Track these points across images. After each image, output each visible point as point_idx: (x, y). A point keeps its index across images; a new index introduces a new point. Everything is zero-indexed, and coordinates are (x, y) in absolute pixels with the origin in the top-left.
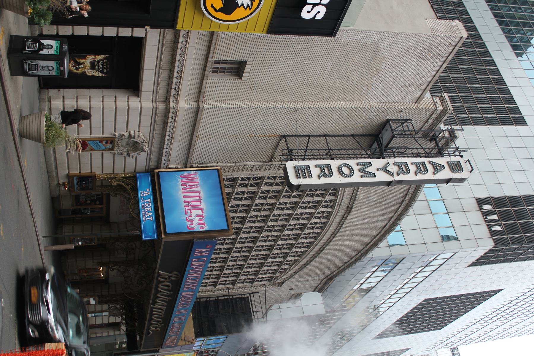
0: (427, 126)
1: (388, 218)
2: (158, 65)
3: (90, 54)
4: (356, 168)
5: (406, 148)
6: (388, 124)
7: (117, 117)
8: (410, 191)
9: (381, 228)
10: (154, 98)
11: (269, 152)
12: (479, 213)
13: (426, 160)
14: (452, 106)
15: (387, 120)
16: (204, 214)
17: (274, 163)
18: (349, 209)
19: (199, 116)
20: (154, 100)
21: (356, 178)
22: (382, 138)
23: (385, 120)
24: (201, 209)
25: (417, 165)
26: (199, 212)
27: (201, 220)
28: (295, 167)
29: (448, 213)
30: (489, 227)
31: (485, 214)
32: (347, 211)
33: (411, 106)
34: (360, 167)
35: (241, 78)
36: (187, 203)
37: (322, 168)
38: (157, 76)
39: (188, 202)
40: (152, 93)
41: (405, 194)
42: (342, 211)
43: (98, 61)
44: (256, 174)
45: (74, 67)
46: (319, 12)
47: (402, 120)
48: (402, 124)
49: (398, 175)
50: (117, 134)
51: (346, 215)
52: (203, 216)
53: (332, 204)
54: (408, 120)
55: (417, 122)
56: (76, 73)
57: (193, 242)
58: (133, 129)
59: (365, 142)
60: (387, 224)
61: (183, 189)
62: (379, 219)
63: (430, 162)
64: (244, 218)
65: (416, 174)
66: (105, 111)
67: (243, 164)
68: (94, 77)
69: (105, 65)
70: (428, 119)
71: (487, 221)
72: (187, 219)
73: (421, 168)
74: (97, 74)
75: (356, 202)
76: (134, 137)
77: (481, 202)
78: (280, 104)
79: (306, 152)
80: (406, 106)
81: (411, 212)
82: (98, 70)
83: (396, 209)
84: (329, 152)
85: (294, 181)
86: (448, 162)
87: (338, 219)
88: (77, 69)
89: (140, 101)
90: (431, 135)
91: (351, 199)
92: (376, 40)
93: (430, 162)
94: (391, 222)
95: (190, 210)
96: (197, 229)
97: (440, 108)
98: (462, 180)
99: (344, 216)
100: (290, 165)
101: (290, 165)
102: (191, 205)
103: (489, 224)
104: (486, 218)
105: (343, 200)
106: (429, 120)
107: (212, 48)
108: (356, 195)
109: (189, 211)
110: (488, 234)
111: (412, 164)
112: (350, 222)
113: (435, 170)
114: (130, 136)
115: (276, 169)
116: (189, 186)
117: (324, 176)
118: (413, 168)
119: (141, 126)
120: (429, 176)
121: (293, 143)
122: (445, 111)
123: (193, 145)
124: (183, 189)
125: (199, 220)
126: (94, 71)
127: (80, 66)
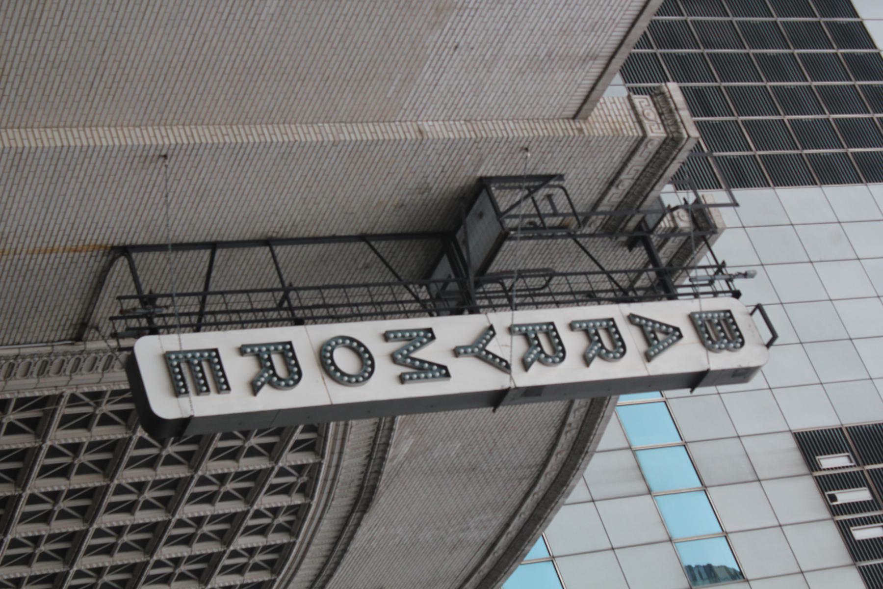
0: (615, 195)
1: (501, 517)
4: (380, 350)
5: (550, 274)
6: (484, 194)
8: (571, 419)
9: (479, 555)
11: (71, 309)
12: (808, 485)
13: (618, 312)
14: (699, 126)
15: (481, 179)
17: (91, 346)
18: (364, 496)
21: (384, 385)
22: (466, 242)
25: (589, 331)
28: (166, 357)
29: (704, 488)
30: (844, 529)
31: (828, 484)
32: (357, 500)
33: (562, 128)
34: (393, 346)
37: (260, 355)
41: (553, 431)
47: (530, 178)
48: (532, 191)
49: (526, 366)
51: (355, 516)
53: (304, 478)
54: (550, 177)
55: (582, 184)
59: (408, 258)
60: (498, 538)
62: (472, 525)
63: (631, 318)
64: (75, 538)
65: (587, 361)
71: (835, 510)
73: (603, 341)
75: (388, 467)
77: (812, 445)
78: (105, 137)
79: (203, 303)
80: (540, 130)
81: (578, 491)
83: (525, 485)
84: (286, 297)
85: (165, 405)
86: (691, 317)
90: (632, 224)
91: (370, 457)
93: (631, 318)
97: (656, 132)
98: (741, 375)
99: (347, 519)
100: (149, 350)
101: (149, 350)
103: (844, 518)
104: (833, 498)
105: (344, 464)
106: (623, 176)
108: (387, 444)
110: (841, 554)
111: (572, 326)
112: (369, 541)
113: (649, 342)
115: (101, 365)
117: (270, 383)
118: (574, 343)
120: (631, 365)
121: (155, 272)
122: (672, 142)
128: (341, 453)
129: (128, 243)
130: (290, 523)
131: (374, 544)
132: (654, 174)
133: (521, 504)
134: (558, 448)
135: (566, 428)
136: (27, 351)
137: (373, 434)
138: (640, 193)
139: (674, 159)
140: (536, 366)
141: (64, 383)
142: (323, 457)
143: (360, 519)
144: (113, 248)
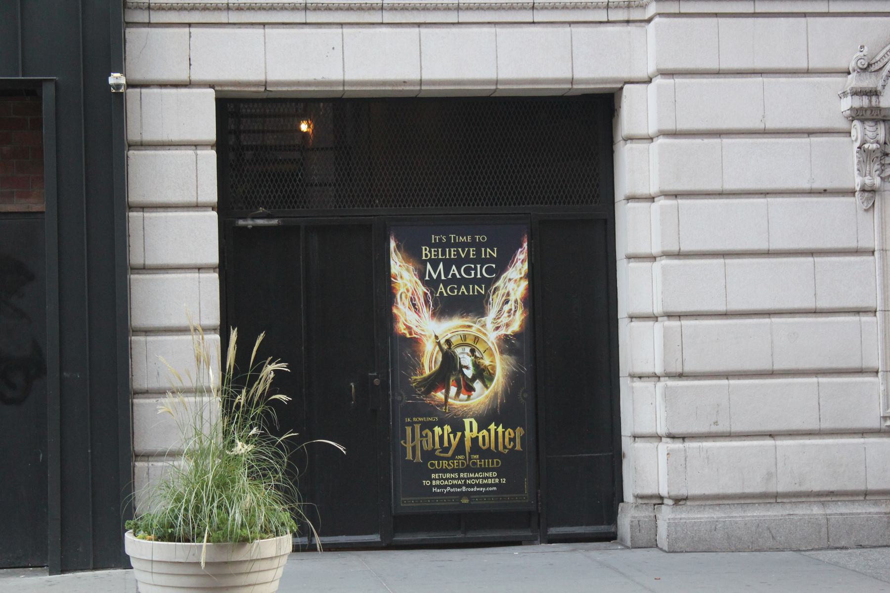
2: (388, 17)
3: (392, 319)
7: (729, 186)
10: (621, 15)
20: (636, 15)
38: (465, 17)
40: (499, 30)
43: (431, 284)
45: (470, 389)
50: (857, 182)
56: (514, 380)
58: (832, 103)
66: (686, 247)
68: (532, 300)
69: (452, 253)
74: (514, 282)
76: (873, 93)
82: (489, 283)
88: (483, 374)
89: (649, 81)
114: (858, 115)
119: (803, 65)
126: (496, 301)
127: (466, 360)
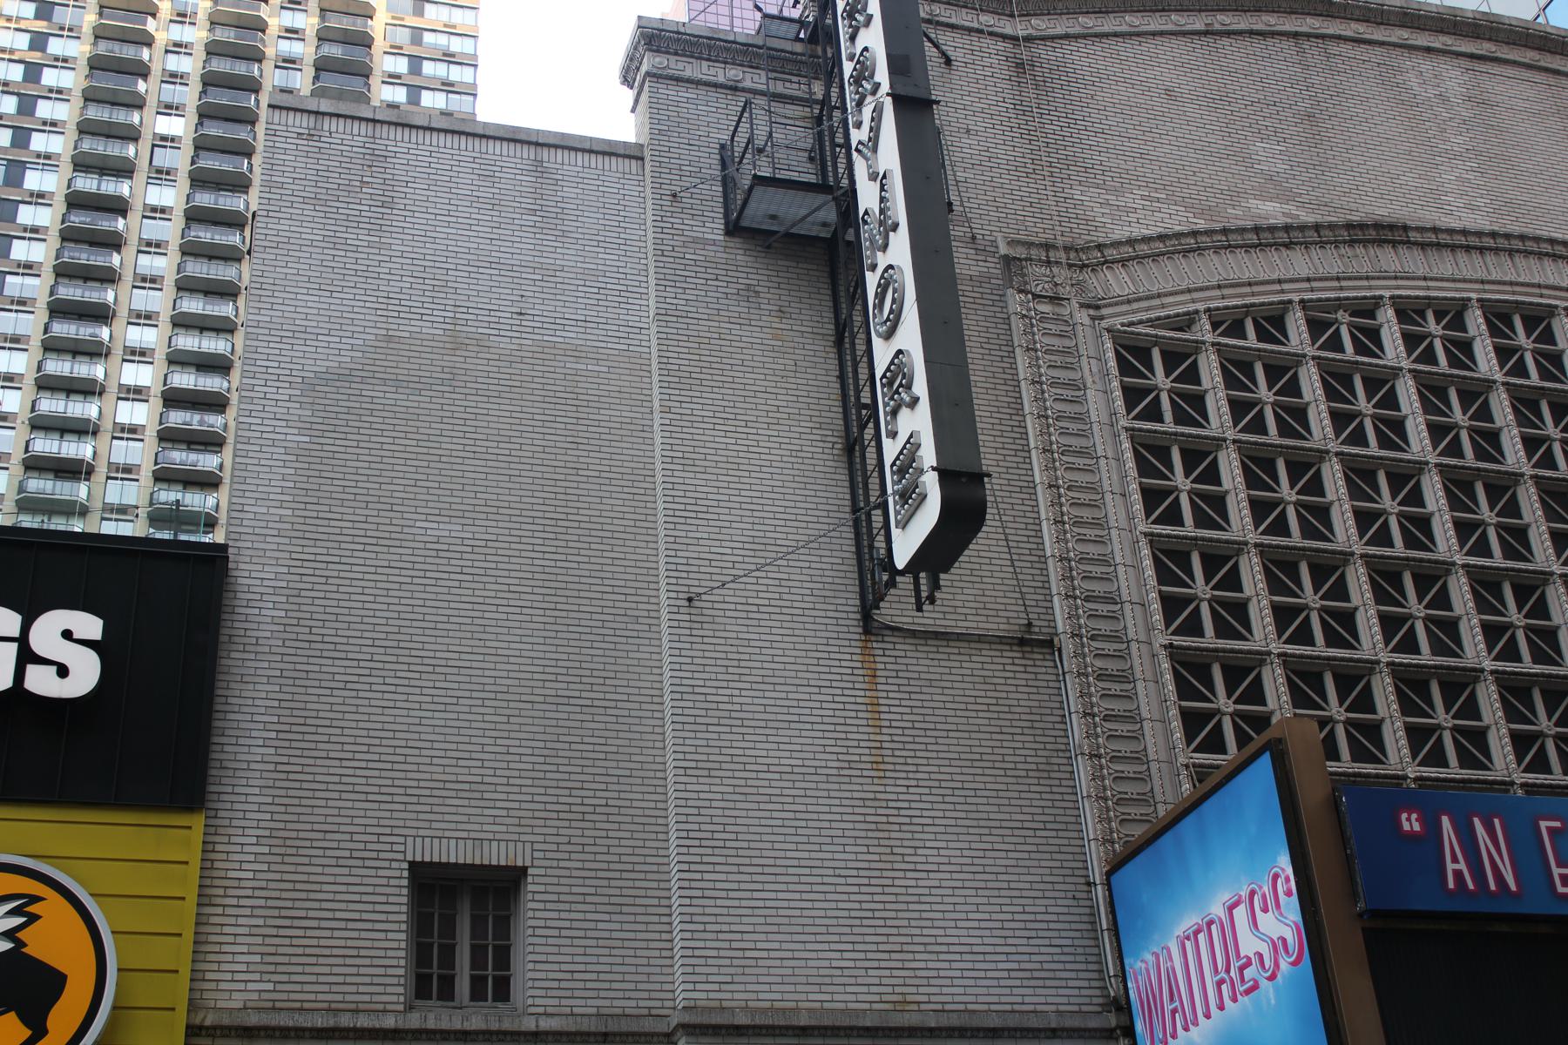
1: (1409, 62)
6: (745, 223)
8: (1199, 26)
11: (997, 665)
16: (1244, 893)
19: (742, 1020)
23: (736, 242)
24: (1231, 908)
26: (1241, 913)
27: (1264, 896)
32: (1380, 242)
34: (879, 254)
35: (524, 870)
36: (1224, 987)
39: (1220, 983)
41: (1226, 41)
42: (1389, 259)
44: (1156, 696)
46: (67, 635)
52: (1253, 893)
53: (1344, 317)
57: (1374, 914)
61: (1186, 1029)
62: (1432, 92)
67: (1083, 769)
70: (722, 86)
72: (1272, 978)
75: (1308, 218)
87: (1445, 265)
90: (799, 48)
91: (1287, 246)
92: (284, 394)
94: (1438, 41)
95: (1242, 969)
96: (1292, 909)
99: (1423, 246)
102: (1228, 971)
105: (1304, 273)
106: (721, 79)
107: (320, 1021)
109: (1248, 973)
116: (1172, 1000)
123: (955, 1021)
124: (1186, 1029)
125: (1265, 910)
128: (1280, 282)
129: (858, 616)
130: (1439, 316)
131: (1480, 202)
132: (710, 47)
133: (1382, 44)
134: (1260, 27)
135: (1217, 27)
136: (1074, 704)
137: (1240, 253)
138: (745, 53)
139: (678, 33)
140: (877, 79)
141: (1144, 648)
142: (1290, 302)
143: (1417, 229)
144: (867, 631)
